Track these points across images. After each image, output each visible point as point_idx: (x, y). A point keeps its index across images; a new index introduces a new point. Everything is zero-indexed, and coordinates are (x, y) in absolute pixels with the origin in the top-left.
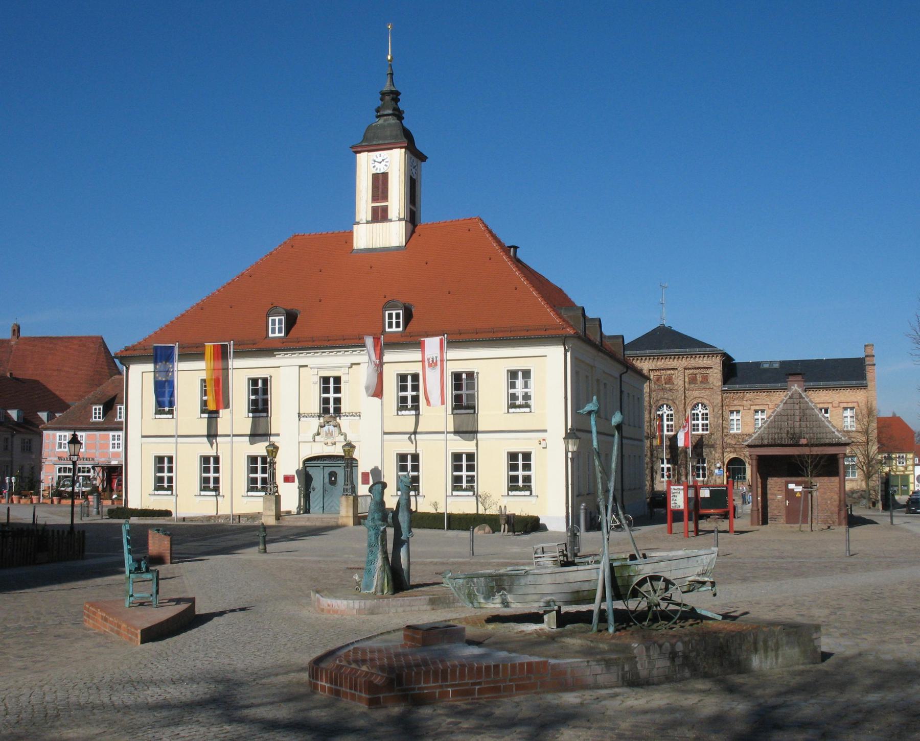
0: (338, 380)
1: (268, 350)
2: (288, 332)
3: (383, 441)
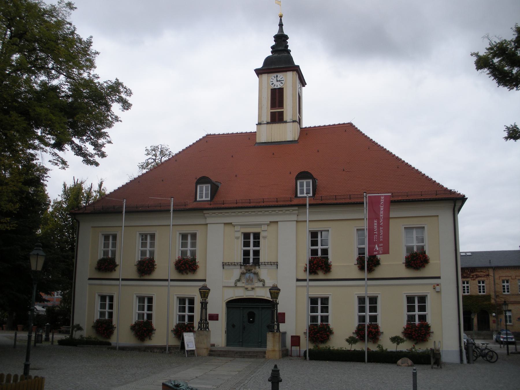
0: (257, 236)
1: (200, 209)
2: (212, 197)
3: (297, 286)
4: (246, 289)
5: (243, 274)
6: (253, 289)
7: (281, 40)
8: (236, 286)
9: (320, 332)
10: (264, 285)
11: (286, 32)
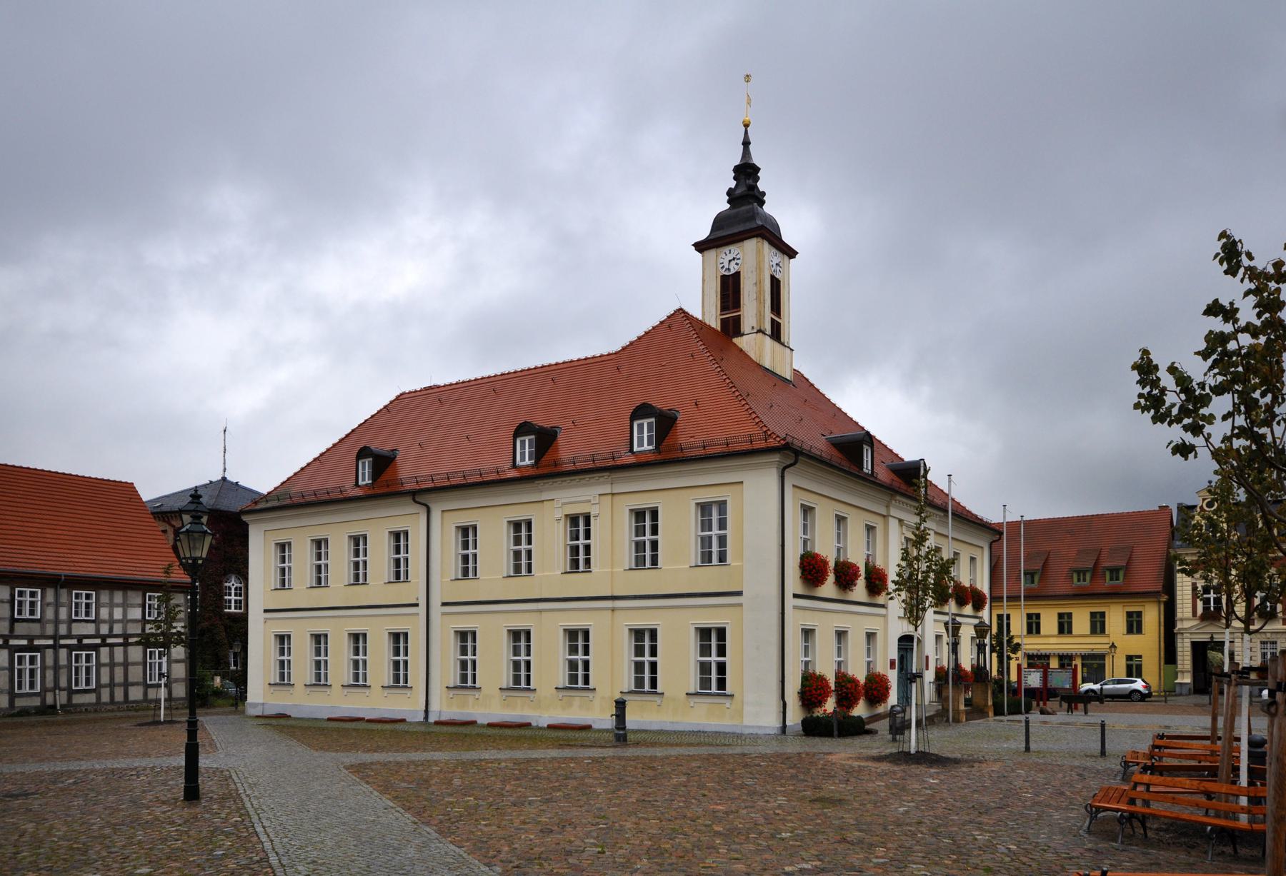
7: (746, 172)
11: (756, 159)
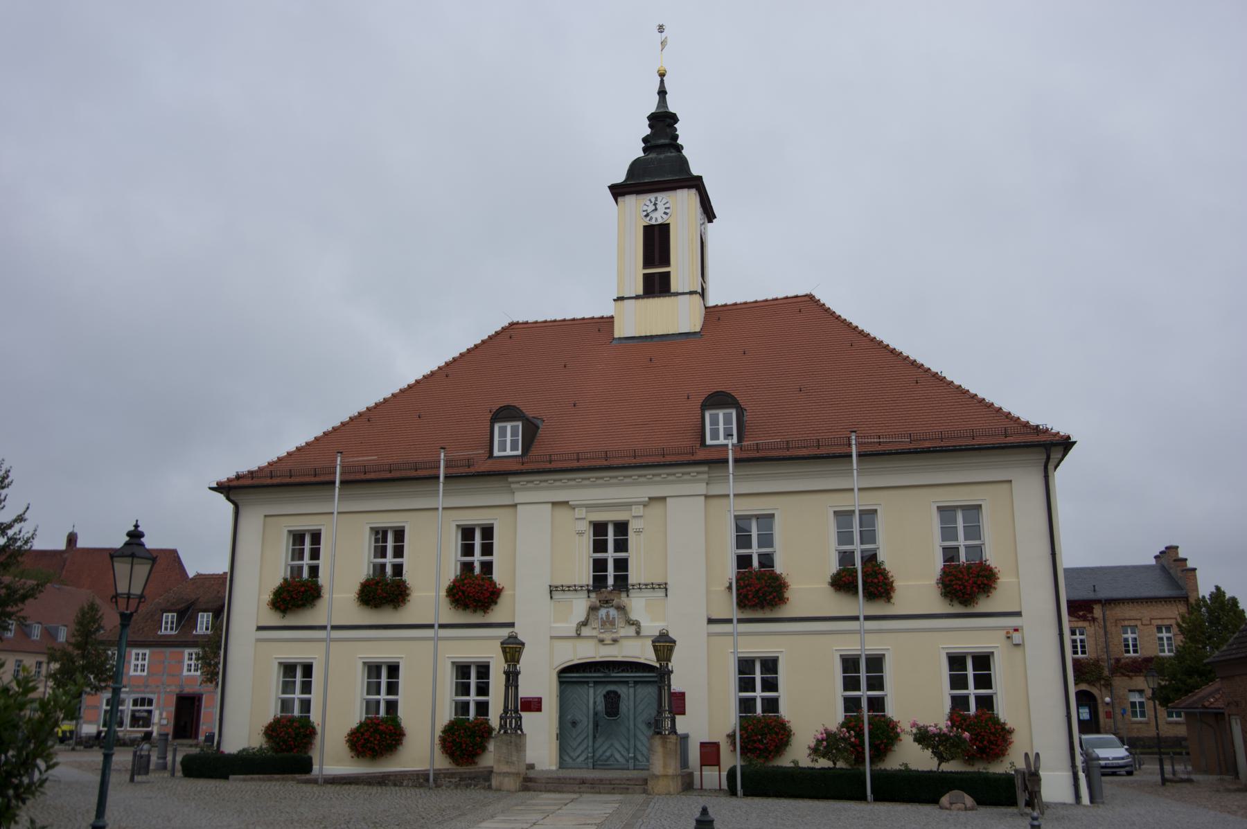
0: (622, 528)
1: (500, 474)
2: (526, 449)
3: (709, 635)
4: (601, 641)
5: (593, 609)
6: (615, 641)
8: (579, 636)
9: (762, 732)
10: (638, 633)
